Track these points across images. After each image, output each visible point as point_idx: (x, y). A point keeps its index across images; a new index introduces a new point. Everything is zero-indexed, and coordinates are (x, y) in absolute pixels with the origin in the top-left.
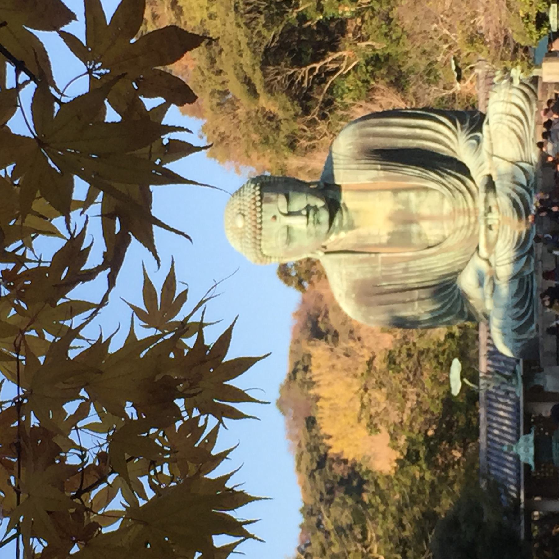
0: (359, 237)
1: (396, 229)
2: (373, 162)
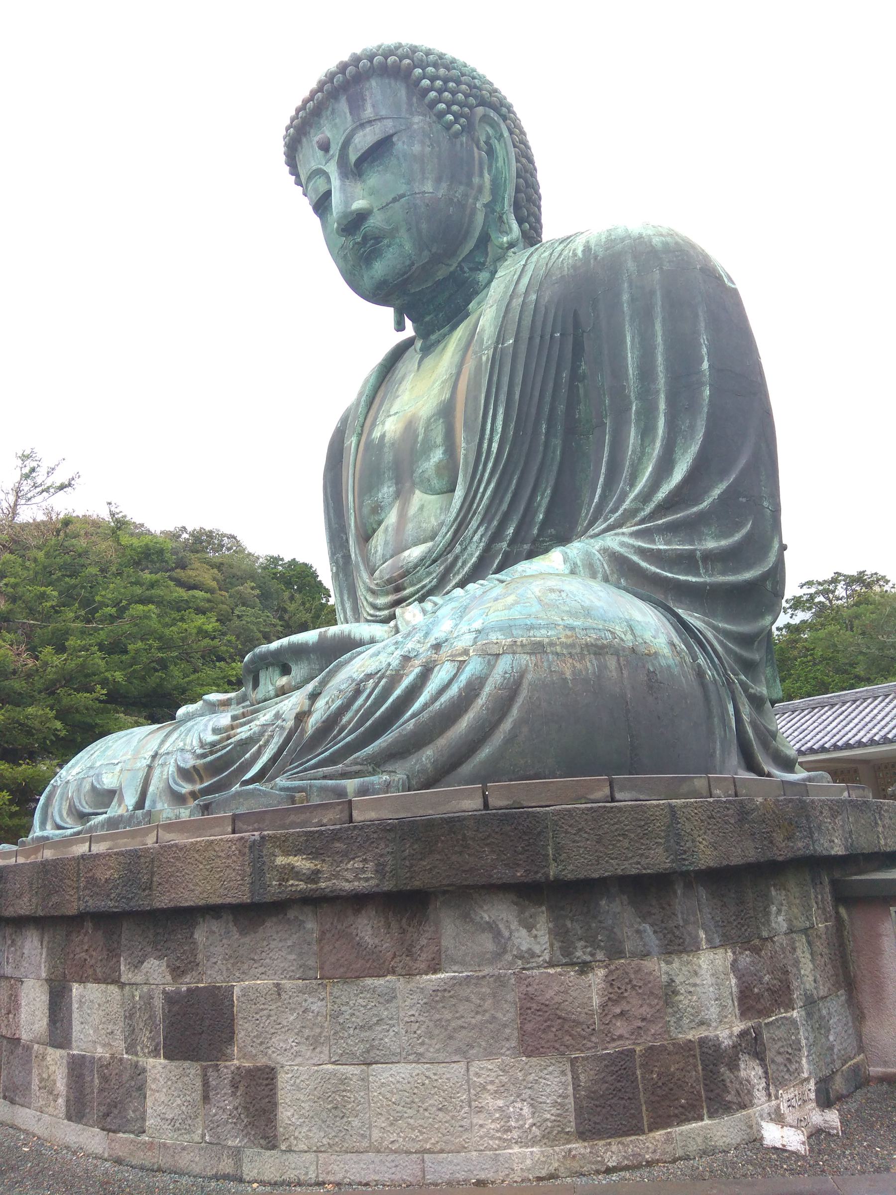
0: (403, 378)
1: (386, 450)
2: (527, 322)
